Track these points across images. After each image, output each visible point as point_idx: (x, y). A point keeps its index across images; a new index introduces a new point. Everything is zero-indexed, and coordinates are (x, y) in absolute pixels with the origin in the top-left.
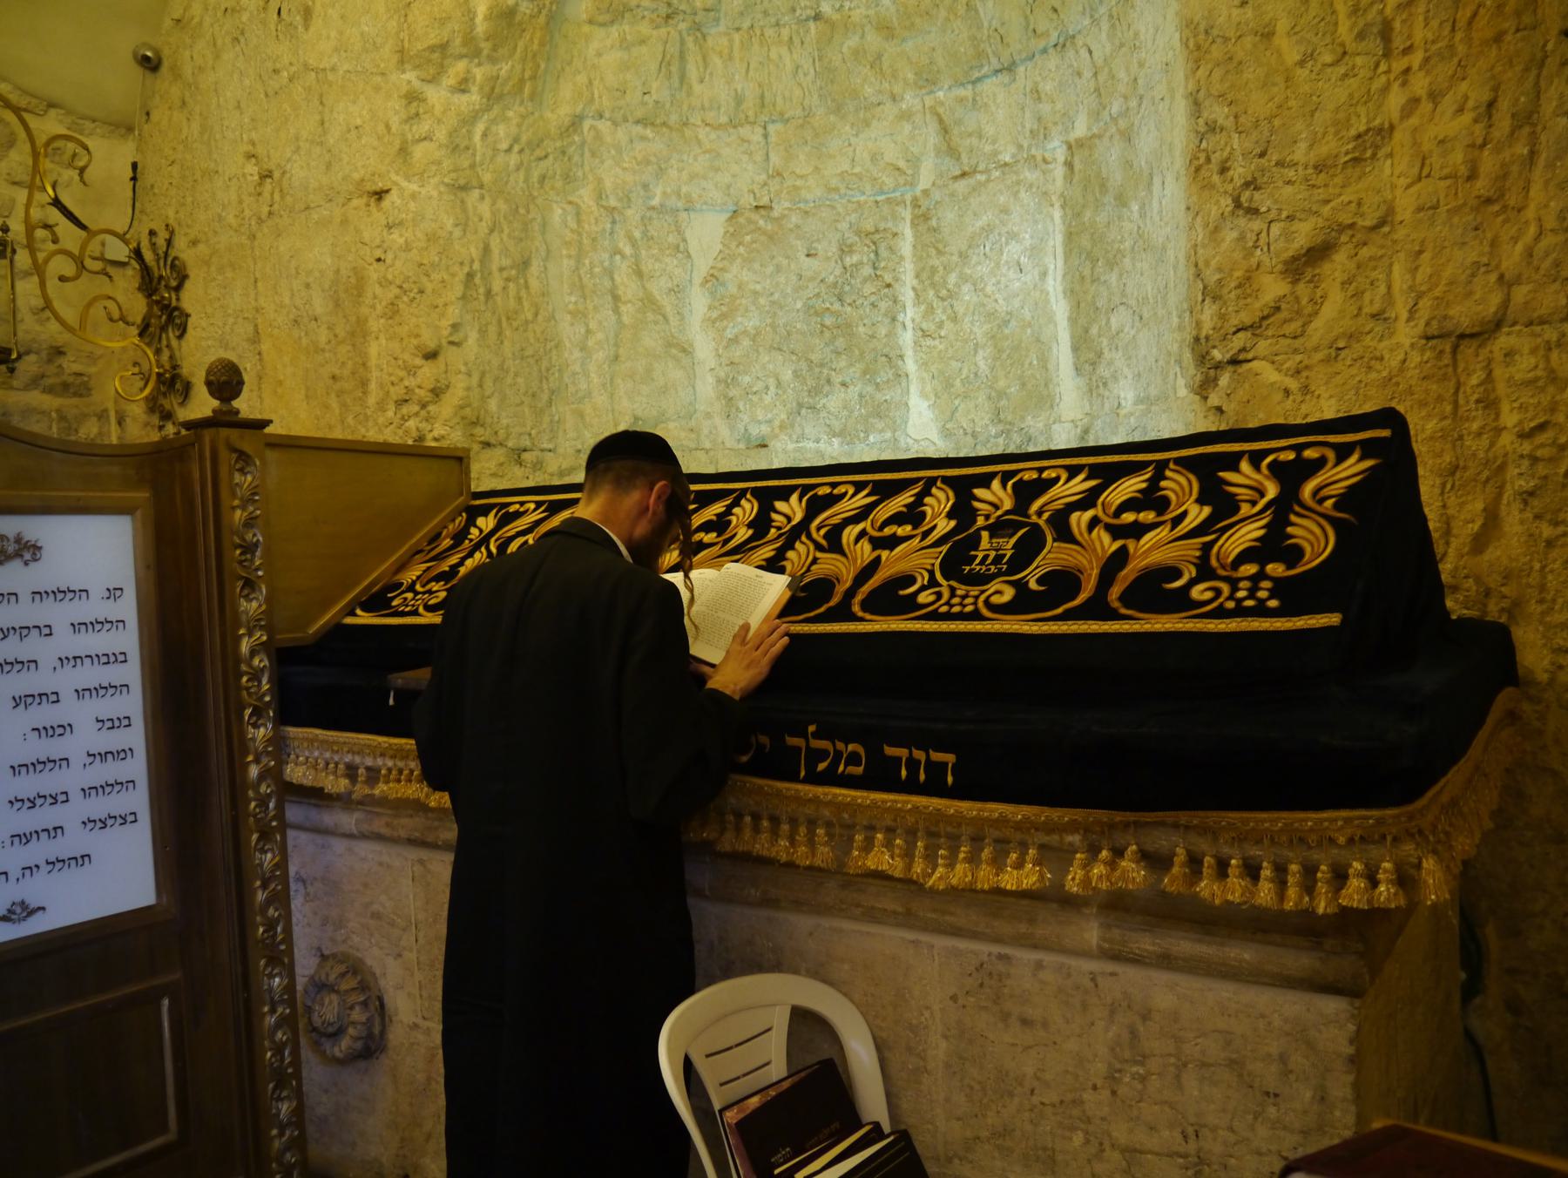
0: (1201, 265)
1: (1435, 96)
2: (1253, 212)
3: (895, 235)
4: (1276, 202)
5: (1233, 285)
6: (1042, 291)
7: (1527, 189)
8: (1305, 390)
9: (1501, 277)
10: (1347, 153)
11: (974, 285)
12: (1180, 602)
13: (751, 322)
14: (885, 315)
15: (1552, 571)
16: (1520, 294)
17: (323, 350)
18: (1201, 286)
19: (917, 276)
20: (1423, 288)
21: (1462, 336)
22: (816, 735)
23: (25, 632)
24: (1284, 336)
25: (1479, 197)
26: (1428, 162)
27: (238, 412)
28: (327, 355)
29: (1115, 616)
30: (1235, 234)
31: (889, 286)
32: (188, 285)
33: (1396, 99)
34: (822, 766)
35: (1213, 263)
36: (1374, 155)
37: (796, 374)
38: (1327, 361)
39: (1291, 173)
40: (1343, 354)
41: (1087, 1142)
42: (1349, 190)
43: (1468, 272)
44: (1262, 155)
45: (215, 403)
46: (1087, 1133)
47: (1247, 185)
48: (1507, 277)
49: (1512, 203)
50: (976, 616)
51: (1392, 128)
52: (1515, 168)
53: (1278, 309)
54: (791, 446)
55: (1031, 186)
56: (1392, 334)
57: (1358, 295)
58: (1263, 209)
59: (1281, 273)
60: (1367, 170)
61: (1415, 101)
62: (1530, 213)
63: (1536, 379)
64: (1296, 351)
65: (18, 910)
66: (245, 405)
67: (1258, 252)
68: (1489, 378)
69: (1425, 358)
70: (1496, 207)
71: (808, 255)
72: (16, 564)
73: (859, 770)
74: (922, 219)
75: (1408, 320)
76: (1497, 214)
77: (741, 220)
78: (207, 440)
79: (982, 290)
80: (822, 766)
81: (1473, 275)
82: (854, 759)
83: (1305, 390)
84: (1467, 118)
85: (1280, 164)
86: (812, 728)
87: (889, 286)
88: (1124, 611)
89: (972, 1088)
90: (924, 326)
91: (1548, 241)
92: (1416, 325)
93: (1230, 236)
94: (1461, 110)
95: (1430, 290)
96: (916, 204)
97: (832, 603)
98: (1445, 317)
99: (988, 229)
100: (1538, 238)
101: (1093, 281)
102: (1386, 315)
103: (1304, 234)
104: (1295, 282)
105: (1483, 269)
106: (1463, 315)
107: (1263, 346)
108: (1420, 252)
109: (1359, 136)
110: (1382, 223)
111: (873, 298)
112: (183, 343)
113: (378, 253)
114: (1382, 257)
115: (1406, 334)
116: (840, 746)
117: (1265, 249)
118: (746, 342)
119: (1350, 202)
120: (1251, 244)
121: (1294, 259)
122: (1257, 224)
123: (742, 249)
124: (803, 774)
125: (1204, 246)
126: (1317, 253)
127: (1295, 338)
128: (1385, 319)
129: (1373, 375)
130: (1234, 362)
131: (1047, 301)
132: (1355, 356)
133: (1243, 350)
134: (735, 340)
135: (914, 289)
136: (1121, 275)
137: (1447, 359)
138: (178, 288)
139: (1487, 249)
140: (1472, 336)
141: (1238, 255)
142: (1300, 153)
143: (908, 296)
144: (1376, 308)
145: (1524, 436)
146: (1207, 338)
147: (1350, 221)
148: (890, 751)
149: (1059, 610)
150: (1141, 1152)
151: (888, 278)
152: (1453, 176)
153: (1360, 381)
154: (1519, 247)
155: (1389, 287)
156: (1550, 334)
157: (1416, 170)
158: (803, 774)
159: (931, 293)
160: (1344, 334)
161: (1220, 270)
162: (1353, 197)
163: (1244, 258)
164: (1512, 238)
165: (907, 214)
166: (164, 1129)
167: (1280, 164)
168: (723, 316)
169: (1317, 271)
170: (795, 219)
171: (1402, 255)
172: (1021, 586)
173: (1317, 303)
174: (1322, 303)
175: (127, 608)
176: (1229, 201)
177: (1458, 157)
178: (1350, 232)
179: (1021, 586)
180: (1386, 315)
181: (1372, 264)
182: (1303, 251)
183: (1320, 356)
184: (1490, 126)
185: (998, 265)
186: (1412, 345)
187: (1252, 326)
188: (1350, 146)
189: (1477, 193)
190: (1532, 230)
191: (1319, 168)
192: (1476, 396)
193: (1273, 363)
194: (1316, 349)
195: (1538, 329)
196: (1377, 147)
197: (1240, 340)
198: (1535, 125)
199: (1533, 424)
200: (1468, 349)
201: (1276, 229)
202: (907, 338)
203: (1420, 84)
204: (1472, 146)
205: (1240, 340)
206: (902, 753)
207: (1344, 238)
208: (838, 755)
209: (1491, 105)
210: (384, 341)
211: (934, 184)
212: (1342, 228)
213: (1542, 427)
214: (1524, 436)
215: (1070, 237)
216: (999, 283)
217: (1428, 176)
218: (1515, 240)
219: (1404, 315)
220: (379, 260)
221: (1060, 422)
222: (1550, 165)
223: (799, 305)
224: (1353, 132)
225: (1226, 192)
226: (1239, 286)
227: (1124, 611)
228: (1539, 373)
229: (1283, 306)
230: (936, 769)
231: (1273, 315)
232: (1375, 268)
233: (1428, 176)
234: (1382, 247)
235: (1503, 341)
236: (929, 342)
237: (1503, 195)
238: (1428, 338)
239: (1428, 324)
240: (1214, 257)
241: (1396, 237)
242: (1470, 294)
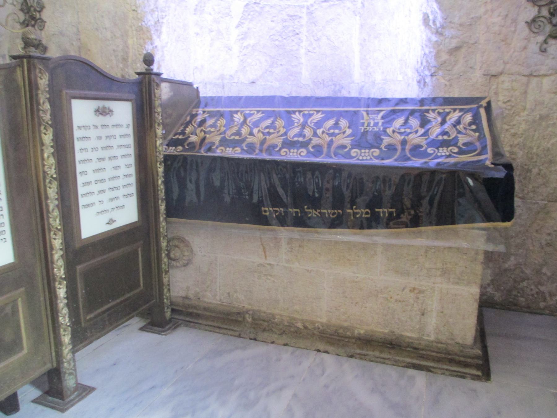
1: (493, 11)
2: (441, 34)
3: (300, 17)
8: (451, 85)
9: (504, 62)
11: (327, 37)
13: (252, 42)
14: (296, 43)
15: (506, 137)
16: (508, 66)
17: (109, 40)
19: (308, 31)
20: (484, 62)
21: (493, 76)
23: (110, 137)
27: (152, 70)
28: (111, 42)
31: (298, 34)
32: (44, 10)
33: (482, 10)
37: (266, 61)
39: (453, 25)
40: (462, 77)
41: (418, 268)
44: (446, 19)
45: (146, 67)
46: (418, 266)
51: (481, 17)
54: (263, 83)
55: (349, 8)
57: (466, 61)
58: (444, 34)
59: (447, 52)
61: (487, 11)
63: (509, 89)
64: (449, 75)
65: (111, 221)
66: (155, 68)
67: (441, 46)
68: (497, 88)
71: (272, 21)
72: (108, 116)
74: (310, 13)
75: (480, 69)
77: (249, 7)
78: (147, 79)
83: (451, 85)
84: (500, 18)
85: (450, 22)
87: (298, 34)
89: (389, 258)
90: (309, 48)
91: (516, 54)
94: (499, 16)
96: (308, 8)
99: (333, 20)
100: (514, 52)
103: (454, 43)
104: (450, 55)
106: (494, 70)
108: (484, 52)
109: (472, 18)
110: (476, 43)
112: (43, 32)
113: (134, 8)
118: (250, 48)
121: (451, 49)
122: (442, 38)
123: (250, 17)
126: (457, 48)
127: (449, 71)
133: (435, 72)
134: (246, 47)
138: (40, 12)
140: (495, 76)
142: (456, 20)
143: (304, 38)
145: (504, 103)
147: (467, 41)
150: (432, 269)
151: (297, 31)
152: (495, 33)
156: (513, 78)
165: (305, 10)
166: (139, 286)
167: (450, 22)
168: (242, 39)
170: (267, 8)
173: (456, 62)
175: (130, 131)
183: (455, 76)
184: (506, 21)
188: (470, 20)
190: (512, 50)
191: (461, 25)
192: (494, 92)
195: (510, 76)
199: (507, 100)
200: (493, 79)
201: (447, 40)
202: (302, 51)
203: (489, 7)
207: (465, 45)
209: (507, 16)
210: (135, 39)
211: (315, 3)
212: (465, 43)
213: (509, 101)
214: (504, 103)
215: (362, 26)
219: (479, 68)
220: (134, 10)
221: (354, 83)
223: (268, 37)
224: (471, 16)
228: (509, 87)
229: (447, 62)
231: (443, 64)
235: (502, 78)
236: (310, 54)
238: (484, 75)
239: (485, 71)
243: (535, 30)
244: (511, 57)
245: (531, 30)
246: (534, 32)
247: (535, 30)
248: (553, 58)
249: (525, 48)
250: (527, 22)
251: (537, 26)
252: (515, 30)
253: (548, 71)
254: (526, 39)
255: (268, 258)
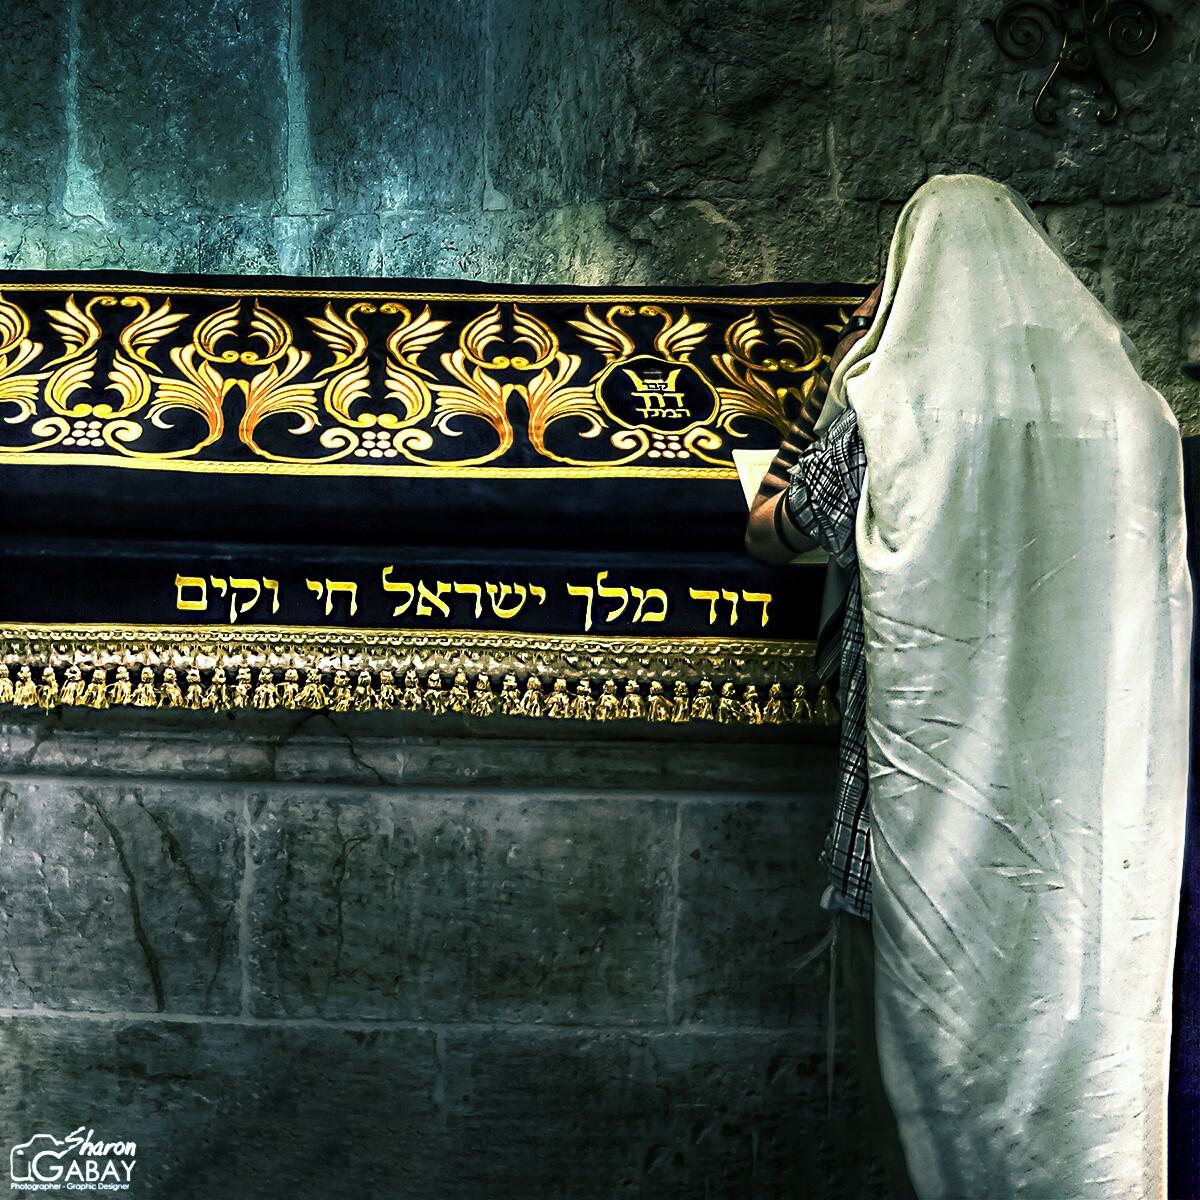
0: (638, 89)
2: (701, 49)
4: (726, 44)
5: (677, 120)
6: (267, 58)
7: (943, 76)
8: (748, 234)
9: (922, 153)
10: (795, 12)
12: (310, 447)
18: (634, 114)
20: (858, 153)
22: (605, 583)
24: (728, 179)
25: (904, 76)
26: (864, 34)
29: (246, 455)
30: (679, 68)
34: (613, 616)
35: (655, 94)
36: (816, 17)
38: (769, 209)
42: (795, 46)
43: (897, 144)
47: (698, 21)
48: (926, 154)
49: (931, 87)
50: (400, 460)
52: (935, 57)
53: (724, 151)
56: (827, 192)
57: (798, 148)
60: (810, 30)
62: (945, 99)
64: (739, 196)
67: (704, 91)
69: (857, 218)
70: (917, 89)
73: (659, 617)
75: (842, 181)
76: (917, 94)
79: (180, 41)
80: (613, 616)
81: (900, 147)
82: (654, 605)
83: (748, 234)
86: (602, 576)
88: (259, 452)
91: (959, 127)
92: (849, 187)
93: (674, 70)
95: (863, 156)
97: (207, 443)
98: (875, 182)
100: (951, 122)
101: (346, 59)
102: (823, 173)
105: (909, 144)
107: (707, 185)
108: (856, 118)
111: (27, 29)
114: (820, 116)
115: (838, 194)
116: (637, 592)
117: (711, 89)
119: (797, 59)
120: (697, 81)
122: (703, 63)
124: (588, 624)
125: (642, 73)
126: (763, 101)
128: (823, 177)
129: (812, 229)
130: (675, 198)
131: (277, 71)
132: (796, 208)
133: (687, 187)
135: (81, 25)
136: (393, 59)
137: (873, 218)
139: (911, 126)
141: (683, 90)
144: (815, 163)
146: (642, 168)
148: (695, 594)
149: (195, 451)
152: (886, 53)
153: (800, 233)
154: (935, 130)
155: (825, 146)
157: (853, 41)
158: (588, 624)
159: (106, 35)
160: (785, 186)
161: (662, 102)
162: (799, 55)
163: (689, 94)
164: (930, 119)
169: (757, 119)
171: (839, 118)
172: (148, 426)
174: (759, 151)
176: (677, 33)
177: (893, 37)
178: (793, 88)
179: (148, 426)
180: (823, 173)
181: (812, 121)
182: (750, 99)
183: (761, 203)
184: (918, 14)
185: (204, 14)
186: (846, 204)
187: (696, 165)
189: (902, 73)
190: (946, 113)
193: (717, 204)
194: (759, 196)
196: (819, 12)
197: (680, 177)
198: (952, 22)
204: (903, 29)
205: (680, 177)
206: (713, 596)
207: (787, 93)
208: (634, 602)
216: (205, 36)
217: (863, 48)
218: (932, 121)
219: (839, 176)
222: (963, 61)
225: (673, 24)
226: (681, 123)
227: (259, 452)
230: (749, 611)
231: (718, 156)
232: (813, 127)
233: (863, 48)
234: (819, 107)
237: (923, 79)
239: (860, 187)
240: (656, 87)
241: (834, 100)
242: (897, 164)
243: (1015, 50)
244: (944, 135)
245: (1000, 46)
246: (1012, 57)
247: (1015, 50)
248: (1077, 146)
249: (986, 108)
250: (987, 22)
251: (1020, 36)
252: (950, 48)
253: (1066, 189)
254: (988, 78)
255: (171, 1000)
